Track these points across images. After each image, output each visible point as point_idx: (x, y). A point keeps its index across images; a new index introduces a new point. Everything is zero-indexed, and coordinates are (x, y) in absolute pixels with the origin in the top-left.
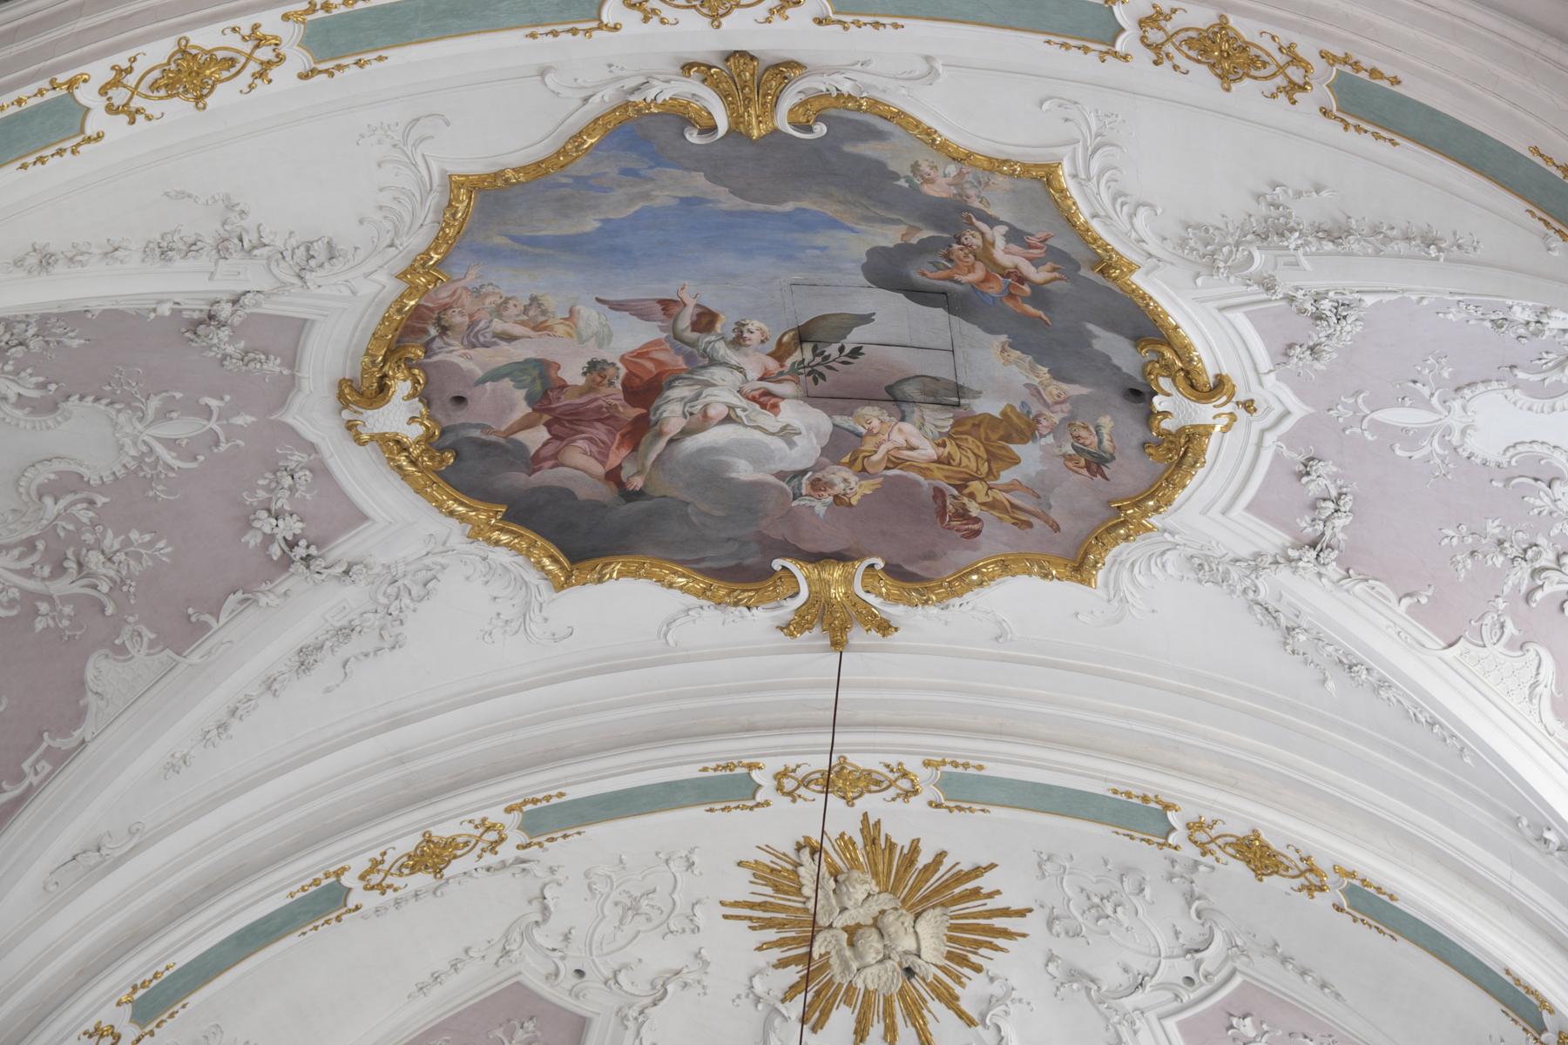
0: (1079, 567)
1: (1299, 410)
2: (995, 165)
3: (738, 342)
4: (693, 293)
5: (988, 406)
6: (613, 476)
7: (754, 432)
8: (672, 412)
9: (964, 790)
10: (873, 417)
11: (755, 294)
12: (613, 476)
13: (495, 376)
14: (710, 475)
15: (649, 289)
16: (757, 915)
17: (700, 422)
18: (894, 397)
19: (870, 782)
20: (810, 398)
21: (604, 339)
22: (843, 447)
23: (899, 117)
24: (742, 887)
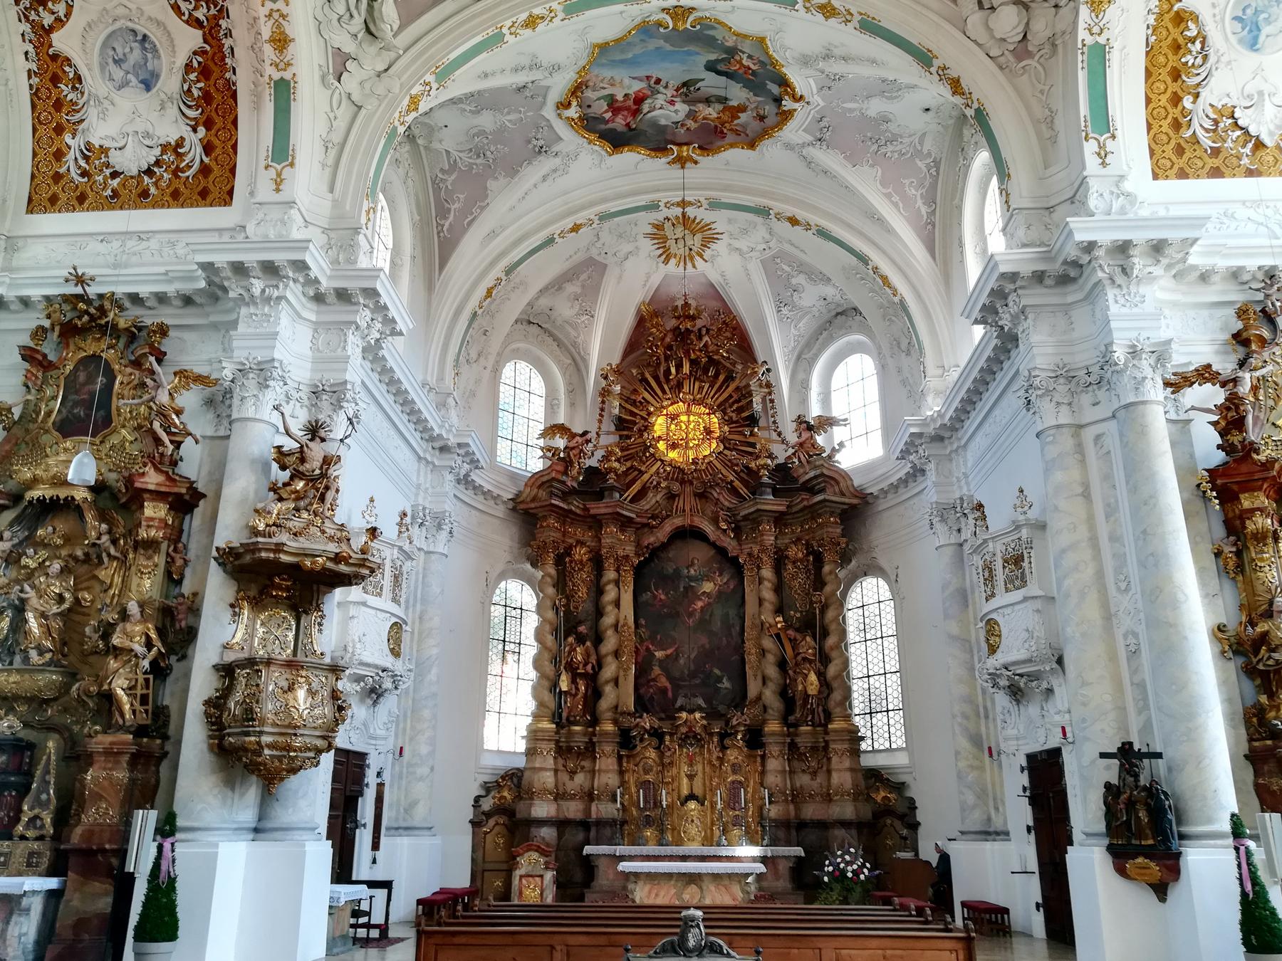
0: (752, 145)
1: (822, 104)
2: (745, 36)
3: (666, 87)
4: (656, 74)
5: (734, 103)
6: (628, 125)
7: (666, 111)
8: (646, 107)
9: (715, 205)
10: (701, 106)
11: (673, 73)
12: (628, 125)
13: (599, 99)
14: (654, 124)
15: (643, 73)
16: (653, 236)
17: (652, 109)
18: (707, 101)
19: (690, 204)
20: (684, 102)
21: (630, 87)
22: (691, 115)
23: (720, 23)
24: (649, 229)
